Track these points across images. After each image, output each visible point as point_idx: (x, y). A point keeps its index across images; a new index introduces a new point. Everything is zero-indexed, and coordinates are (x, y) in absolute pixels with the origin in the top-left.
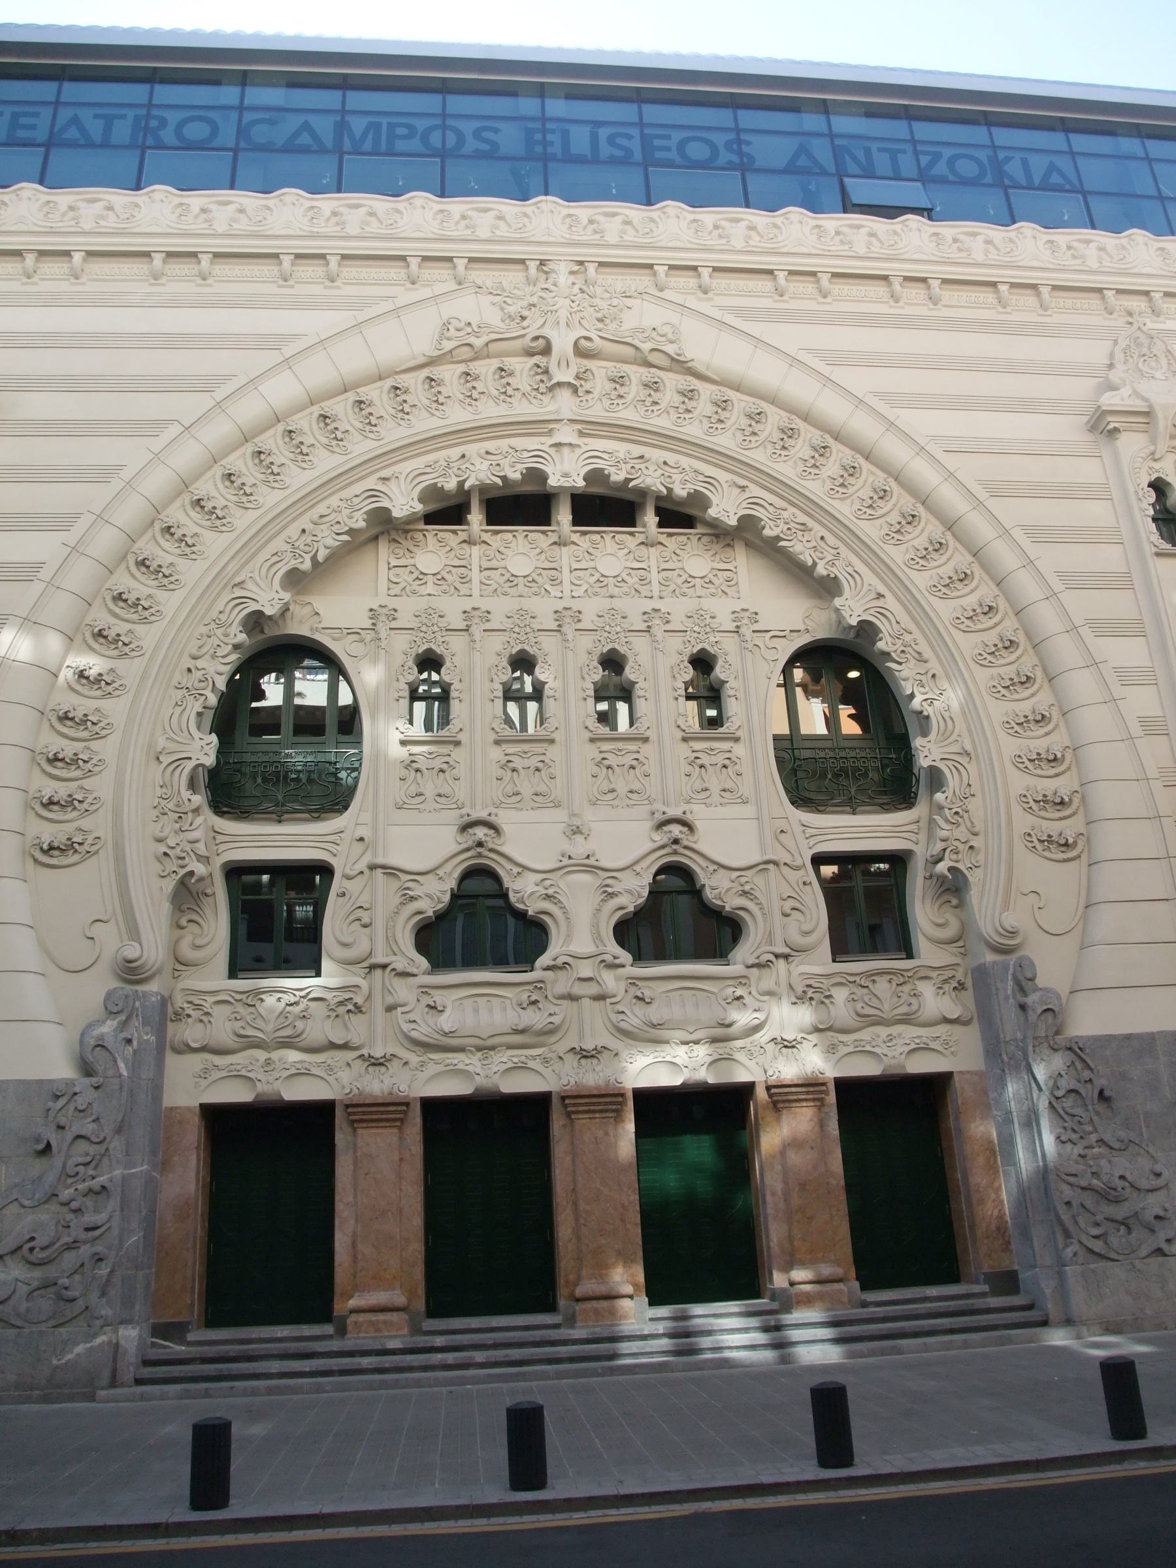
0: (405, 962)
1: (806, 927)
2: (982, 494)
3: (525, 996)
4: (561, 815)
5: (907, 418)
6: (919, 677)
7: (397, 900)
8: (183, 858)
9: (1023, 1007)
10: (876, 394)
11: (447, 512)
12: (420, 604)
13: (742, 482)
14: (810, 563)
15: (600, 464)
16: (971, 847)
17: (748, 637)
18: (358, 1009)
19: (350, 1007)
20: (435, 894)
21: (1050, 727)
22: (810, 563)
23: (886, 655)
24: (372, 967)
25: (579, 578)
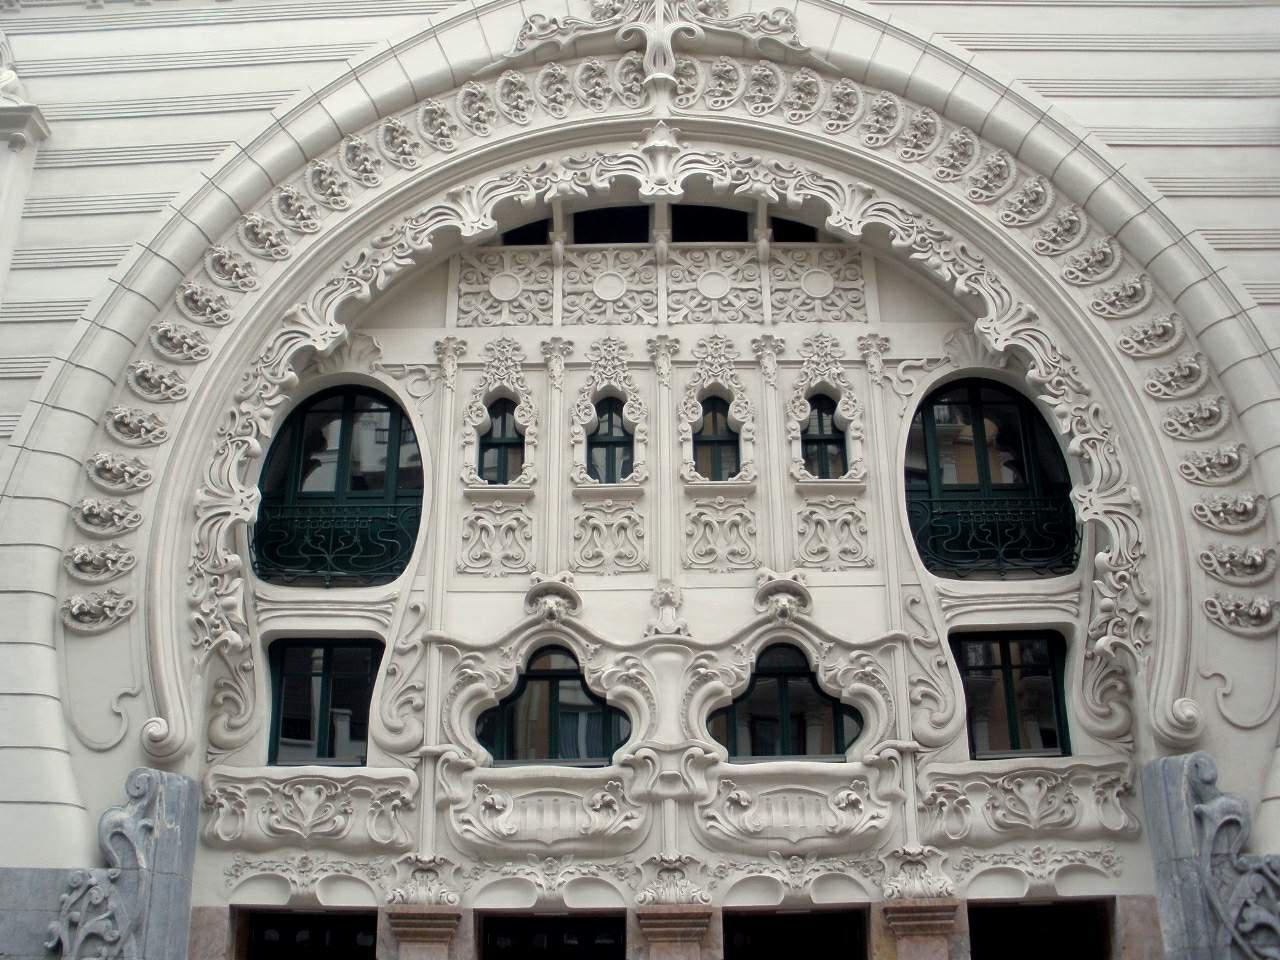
0: (461, 752)
1: (939, 716)
2: (1153, 194)
3: (598, 796)
4: (648, 581)
5: (1060, 109)
6: (1079, 413)
7: (453, 680)
8: (217, 627)
9: (1199, 817)
10: (1027, 82)
11: (526, 233)
12: (491, 335)
13: (867, 186)
14: (948, 278)
15: (701, 169)
16: (1140, 621)
17: (877, 369)
18: (406, 806)
19: (397, 802)
20: (500, 674)
21: (1239, 472)
22: (948, 278)
23: (1040, 386)
24: (423, 758)
25: (678, 302)
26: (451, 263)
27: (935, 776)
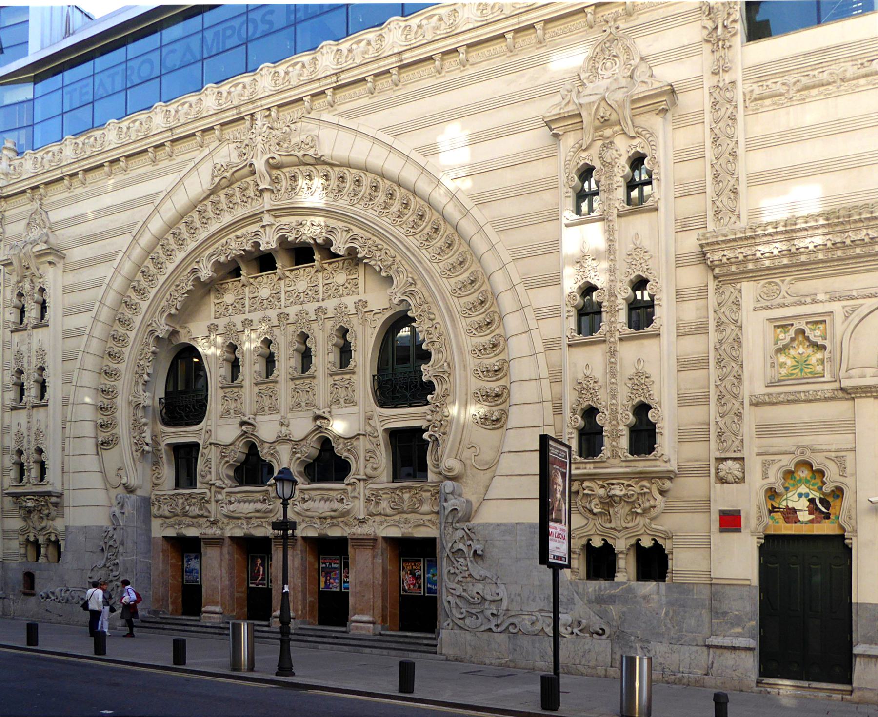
4: (277, 417)
26: (205, 289)
27: (372, 489)
